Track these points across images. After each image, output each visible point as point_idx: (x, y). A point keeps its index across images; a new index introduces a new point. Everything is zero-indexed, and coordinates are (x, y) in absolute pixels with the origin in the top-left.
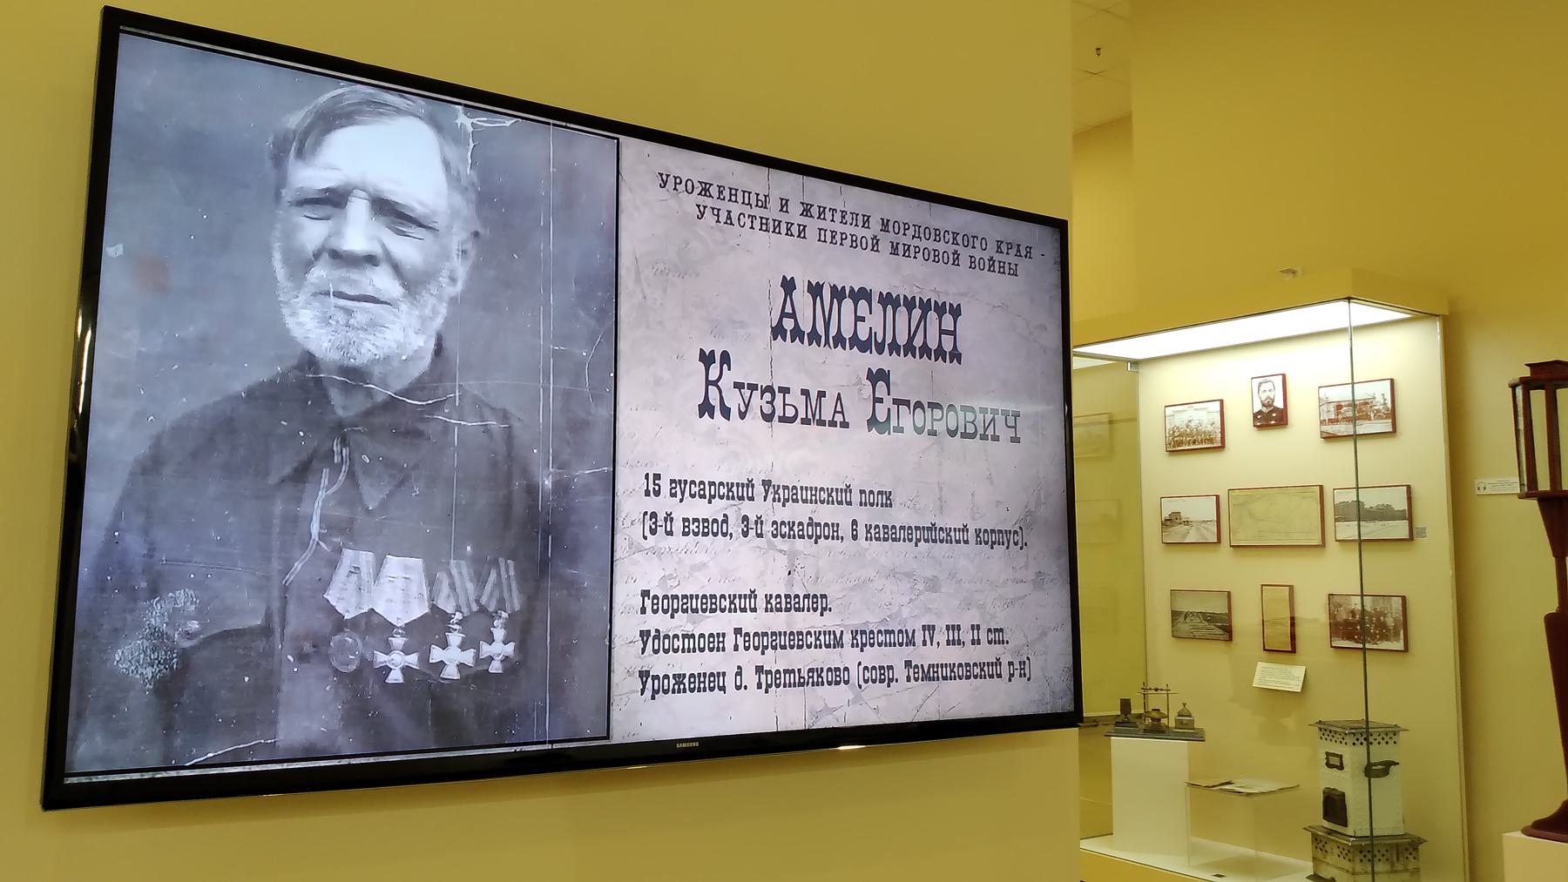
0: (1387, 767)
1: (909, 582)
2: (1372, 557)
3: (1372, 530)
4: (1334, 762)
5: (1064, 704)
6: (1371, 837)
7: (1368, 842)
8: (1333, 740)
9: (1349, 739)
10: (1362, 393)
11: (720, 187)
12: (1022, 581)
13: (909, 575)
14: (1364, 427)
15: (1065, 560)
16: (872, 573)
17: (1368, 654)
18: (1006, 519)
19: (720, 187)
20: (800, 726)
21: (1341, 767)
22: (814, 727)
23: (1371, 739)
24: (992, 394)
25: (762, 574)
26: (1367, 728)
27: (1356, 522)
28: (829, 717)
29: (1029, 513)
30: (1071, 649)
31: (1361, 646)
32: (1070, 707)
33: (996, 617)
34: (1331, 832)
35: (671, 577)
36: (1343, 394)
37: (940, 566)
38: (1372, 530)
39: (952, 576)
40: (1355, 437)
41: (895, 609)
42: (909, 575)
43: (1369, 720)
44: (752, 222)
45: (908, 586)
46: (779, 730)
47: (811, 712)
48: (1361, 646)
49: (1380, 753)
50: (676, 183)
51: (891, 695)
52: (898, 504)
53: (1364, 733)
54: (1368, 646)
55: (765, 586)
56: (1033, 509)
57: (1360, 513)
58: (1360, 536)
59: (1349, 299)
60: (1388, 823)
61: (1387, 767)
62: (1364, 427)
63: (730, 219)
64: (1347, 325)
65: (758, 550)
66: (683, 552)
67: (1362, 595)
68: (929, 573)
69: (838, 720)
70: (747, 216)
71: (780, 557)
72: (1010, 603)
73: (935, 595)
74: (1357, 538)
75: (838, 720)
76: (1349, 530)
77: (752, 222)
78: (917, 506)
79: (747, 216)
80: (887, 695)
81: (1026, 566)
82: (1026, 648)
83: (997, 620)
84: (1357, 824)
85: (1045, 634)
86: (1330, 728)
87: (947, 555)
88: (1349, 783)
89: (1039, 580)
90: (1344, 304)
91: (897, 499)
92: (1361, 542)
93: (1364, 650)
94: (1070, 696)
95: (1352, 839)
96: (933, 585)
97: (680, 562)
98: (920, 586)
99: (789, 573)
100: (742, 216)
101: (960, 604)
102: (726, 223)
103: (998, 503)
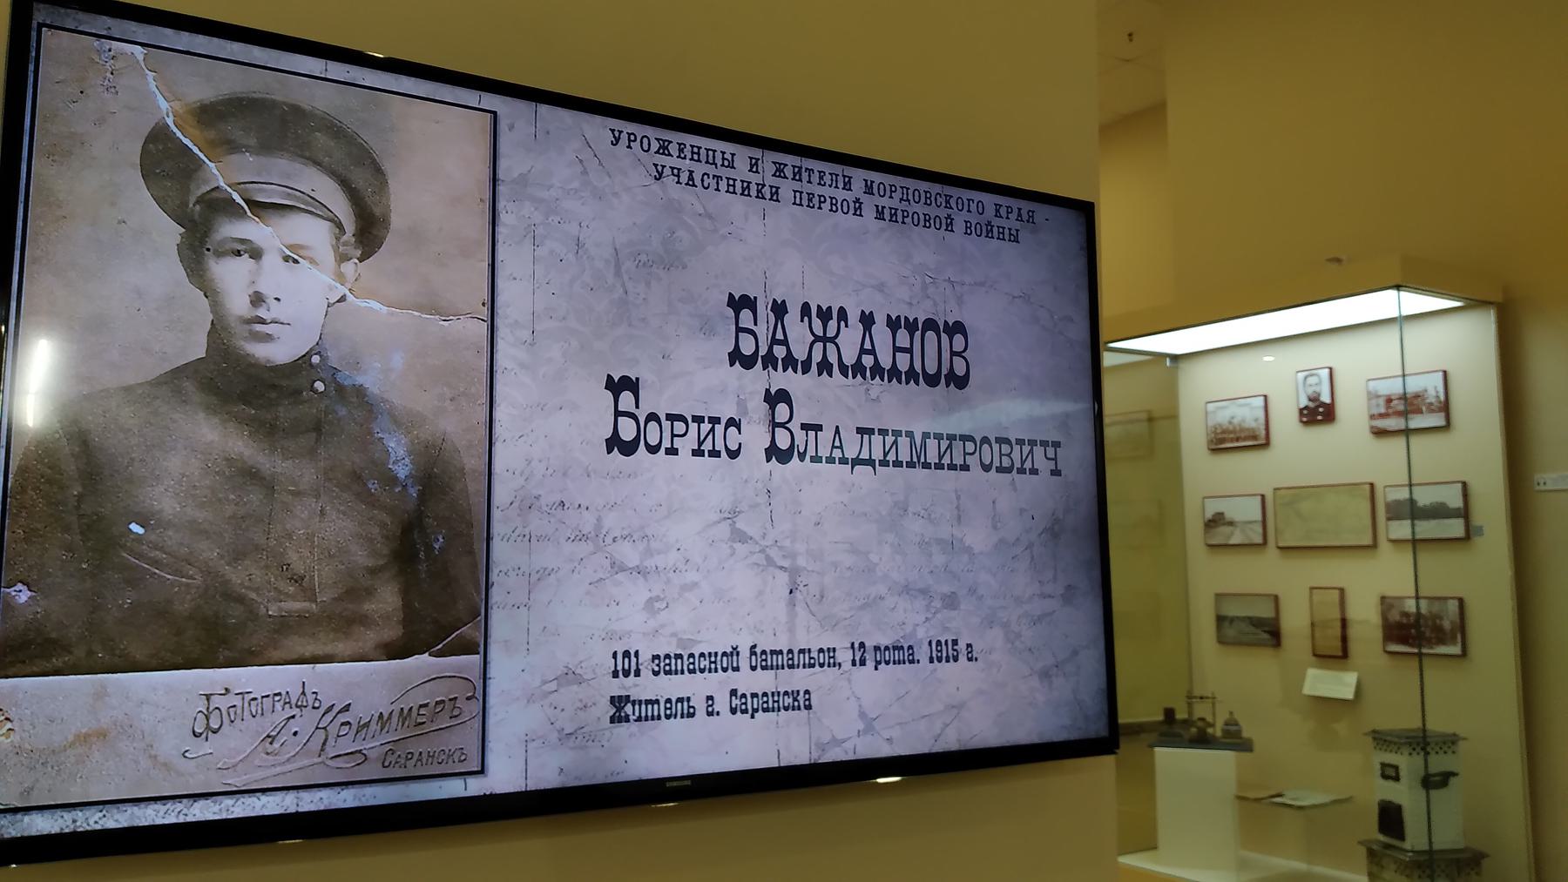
0: (1444, 779)
1: (924, 599)
2: (1427, 559)
3: (1427, 529)
4: (1390, 773)
5: (1098, 729)
6: (1430, 852)
7: (1426, 857)
8: (1389, 749)
9: (1406, 751)
10: (1414, 385)
11: (680, 144)
12: (1050, 596)
13: (924, 592)
14: (1417, 422)
15: (1097, 573)
16: (882, 589)
17: (1426, 661)
18: (1031, 529)
19: (680, 144)
20: (805, 761)
21: (1397, 778)
22: (820, 761)
23: (1428, 749)
24: (1013, 391)
25: (761, 593)
26: (1425, 737)
27: (1409, 522)
28: (837, 750)
29: (1057, 521)
30: (1103, 670)
31: (1416, 651)
32: (1104, 733)
33: (1021, 636)
34: (1387, 846)
35: (658, 599)
36: (1395, 387)
37: (959, 580)
38: (1427, 529)
39: (972, 591)
40: (1407, 432)
41: (909, 629)
42: (924, 592)
43: (1429, 726)
44: (718, 183)
45: (924, 603)
46: (782, 765)
47: (816, 744)
48: (1416, 651)
49: (1439, 763)
50: (630, 140)
51: (906, 723)
52: (910, 515)
53: (1421, 741)
54: (1424, 651)
55: (763, 606)
56: (1061, 517)
57: (1413, 511)
58: (1413, 533)
59: (1398, 287)
60: (1448, 837)
61: (1444, 779)
62: (1417, 422)
63: (693, 180)
64: (1396, 314)
65: (756, 567)
66: (672, 571)
67: (1417, 598)
68: (946, 589)
69: (846, 753)
70: (711, 177)
71: (779, 573)
72: (1037, 621)
73: (954, 613)
74: (1410, 537)
75: (846, 753)
76: (1402, 529)
77: (718, 183)
78: (933, 516)
79: (711, 177)
80: (900, 724)
81: (1055, 579)
82: (1055, 669)
83: (1023, 639)
84: (1415, 838)
85: (1075, 653)
86: (1389, 738)
87: (966, 569)
88: (1404, 794)
89: (1069, 595)
90: (1392, 293)
91: (910, 508)
92: (1415, 543)
93: (1420, 655)
94: (1104, 721)
95: (1410, 854)
96: (951, 602)
97: (668, 581)
98: (937, 604)
99: (791, 592)
100: (706, 177)
101: (982, 623)
102: (687, 184)
103: (1022, 511)
